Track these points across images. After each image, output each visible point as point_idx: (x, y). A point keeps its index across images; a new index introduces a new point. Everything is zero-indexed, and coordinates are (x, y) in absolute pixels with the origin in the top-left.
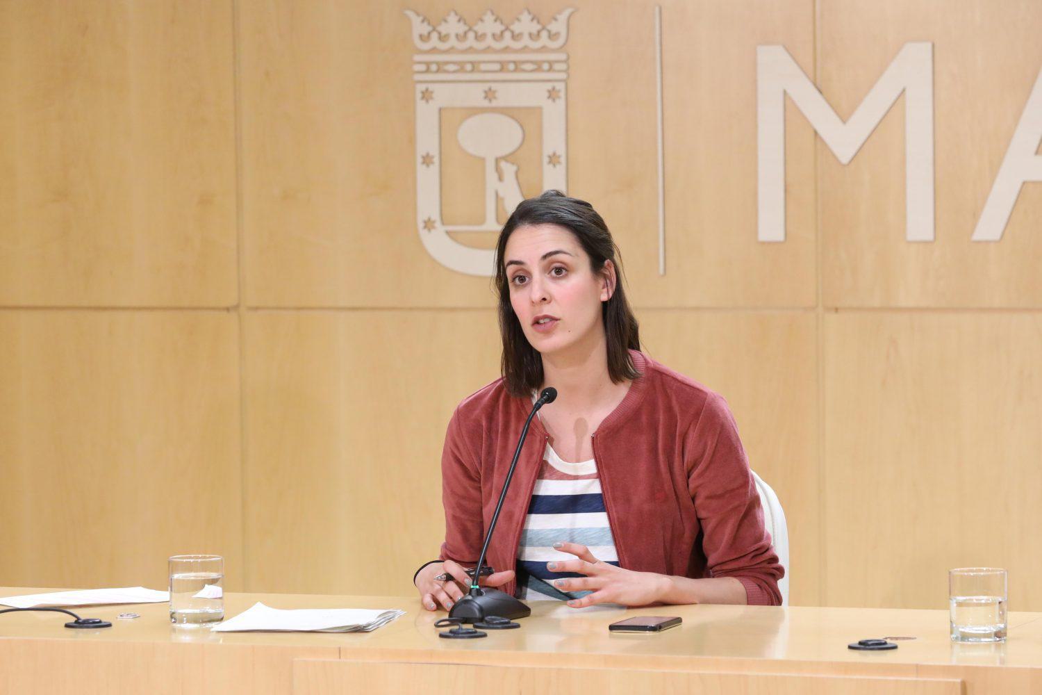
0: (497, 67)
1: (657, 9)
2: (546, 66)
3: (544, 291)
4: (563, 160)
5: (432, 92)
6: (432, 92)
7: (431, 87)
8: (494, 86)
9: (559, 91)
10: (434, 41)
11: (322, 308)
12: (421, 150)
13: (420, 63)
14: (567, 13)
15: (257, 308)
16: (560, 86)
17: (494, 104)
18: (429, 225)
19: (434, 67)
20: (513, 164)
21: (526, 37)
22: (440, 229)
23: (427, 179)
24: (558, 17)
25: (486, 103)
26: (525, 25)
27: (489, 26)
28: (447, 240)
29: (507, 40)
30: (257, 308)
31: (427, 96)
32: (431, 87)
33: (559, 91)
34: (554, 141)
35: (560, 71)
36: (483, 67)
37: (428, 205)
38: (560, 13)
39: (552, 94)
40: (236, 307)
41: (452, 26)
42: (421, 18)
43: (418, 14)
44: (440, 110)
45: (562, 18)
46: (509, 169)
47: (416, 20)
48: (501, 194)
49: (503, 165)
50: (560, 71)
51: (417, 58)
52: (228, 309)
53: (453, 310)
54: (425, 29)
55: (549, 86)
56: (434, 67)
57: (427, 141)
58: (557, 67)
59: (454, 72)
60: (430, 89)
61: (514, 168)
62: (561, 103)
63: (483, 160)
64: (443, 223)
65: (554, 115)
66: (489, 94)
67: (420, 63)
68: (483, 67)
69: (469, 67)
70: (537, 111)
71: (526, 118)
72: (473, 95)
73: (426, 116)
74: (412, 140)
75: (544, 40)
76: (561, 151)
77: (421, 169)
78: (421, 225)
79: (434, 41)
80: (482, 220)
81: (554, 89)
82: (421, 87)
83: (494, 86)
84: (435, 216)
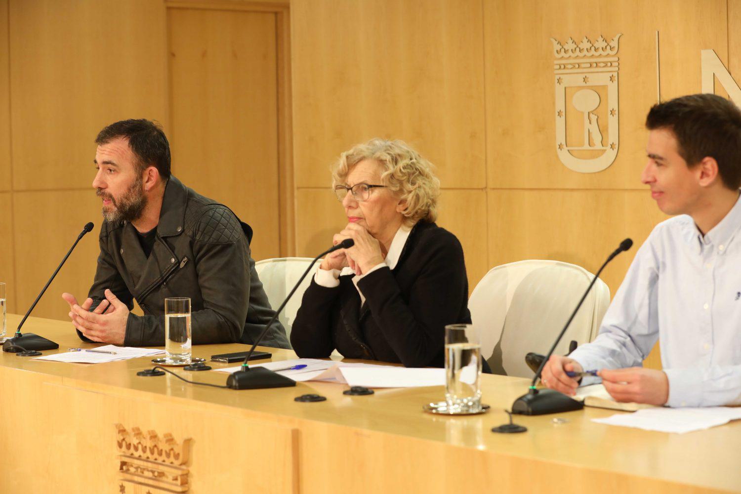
0: (589, 65)
1: (657, 32)
2: (609, 64)
3: (102, 182)
4: (617, 112)
5: (562, 79)
6: (562, 79)
7: (562, 76)
8: (587, 75)
9: (615, 77)
10: (563, 54)
11: (517, 189)
12: (557, 110)
13: (557, 64)
14: (620, 35)
15: (494, 189)
16: (615, 74)
17: (588, 84)
18: (560, 147)
19: (562, 67)
20: (595, 115)
21: (601, 49)
22: (565, 149)
23: (560, 122)
24: (614, 39)
25: (584, 84)
26: (601, 44)
27: (585, 45)
28: (567, 152)
29: (593, 52)
30: (494, 189)
31: (559, 81)
32: (562, 76)
33: (615, 77)
34: (613, 104)
35: (615, 67)
36: (583, 66)
37: (560, 138)
38: (615, 37)
39: (611, 79)
40: (486, 188)
41: (570, 46)
42: (557, 42)
43: (556, 40)
44: (565, 88)
45: (616, 39)
46: (594, 118)
47: (555, 43)
48: (590, 131)
49: (591, 115)
50: (615, 67)
51: (556, 62)
52: (482, 189)
53: (572, 190)
54: (558, 47)
55: (610, 74)
56: (562, 67)
57: (560, 105)
58: (614, 64)
59: (571, 68)
60: (561, 78)
61: (596, 117)
62: (616, 82)
63: (583, 113)
64: (566, 146)
65: (613, 88)
66: (585, 79)
67: (557, 64)
68: (583, 66)
69: (577, 66)
70: (605, 87)
71: (600, 91)
72: (578, 80)
73: (559, 90)
74: (554, 103)
75: (608, 51)
76: (616, 108)
77: (557, 118)
78: (558, 147)
79: (563, 54)
80: (583, 145)
81: (613, 75)
82: (557, 77)
83: (587, 75)
84: (564, 143)
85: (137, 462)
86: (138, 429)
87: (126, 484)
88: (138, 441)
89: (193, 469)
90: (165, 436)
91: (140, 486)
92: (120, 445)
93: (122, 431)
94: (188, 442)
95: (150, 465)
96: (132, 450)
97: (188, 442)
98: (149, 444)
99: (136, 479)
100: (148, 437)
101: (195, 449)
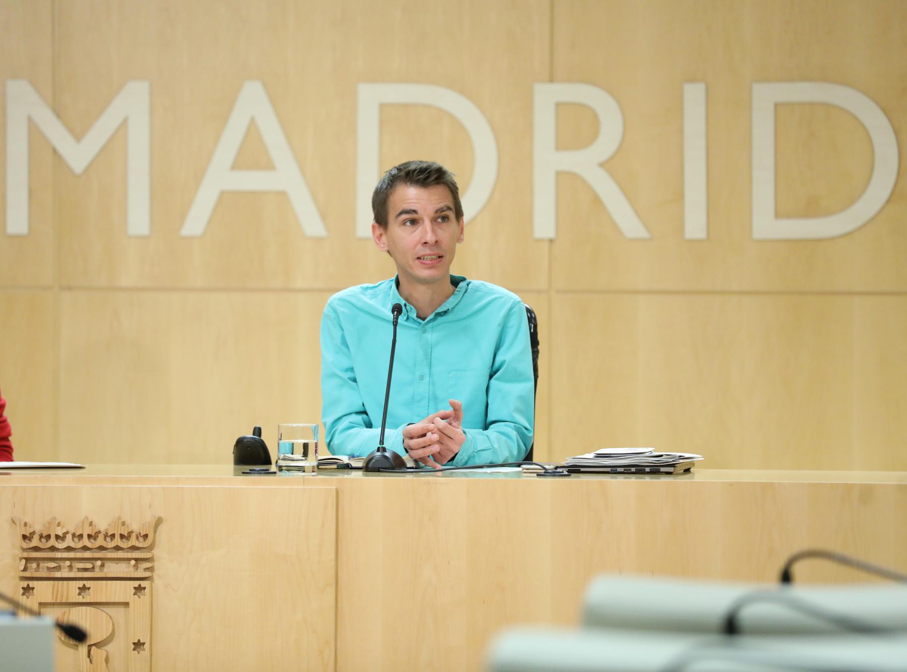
85: (59, 555)
86: (55, 518)
87: (32, 584)
88: (64, 531)
89: (156, 552)
90: (119, 518)
91: (65, 582)
92: (24, 537)
93: (26, 524)
94: (159, 522)
95: (88, 555)
96: (53, 539)
97: (159, 522)
98: (87, 531)
99: (58, 575)
100: (87, 524)
101: (163, 528)
